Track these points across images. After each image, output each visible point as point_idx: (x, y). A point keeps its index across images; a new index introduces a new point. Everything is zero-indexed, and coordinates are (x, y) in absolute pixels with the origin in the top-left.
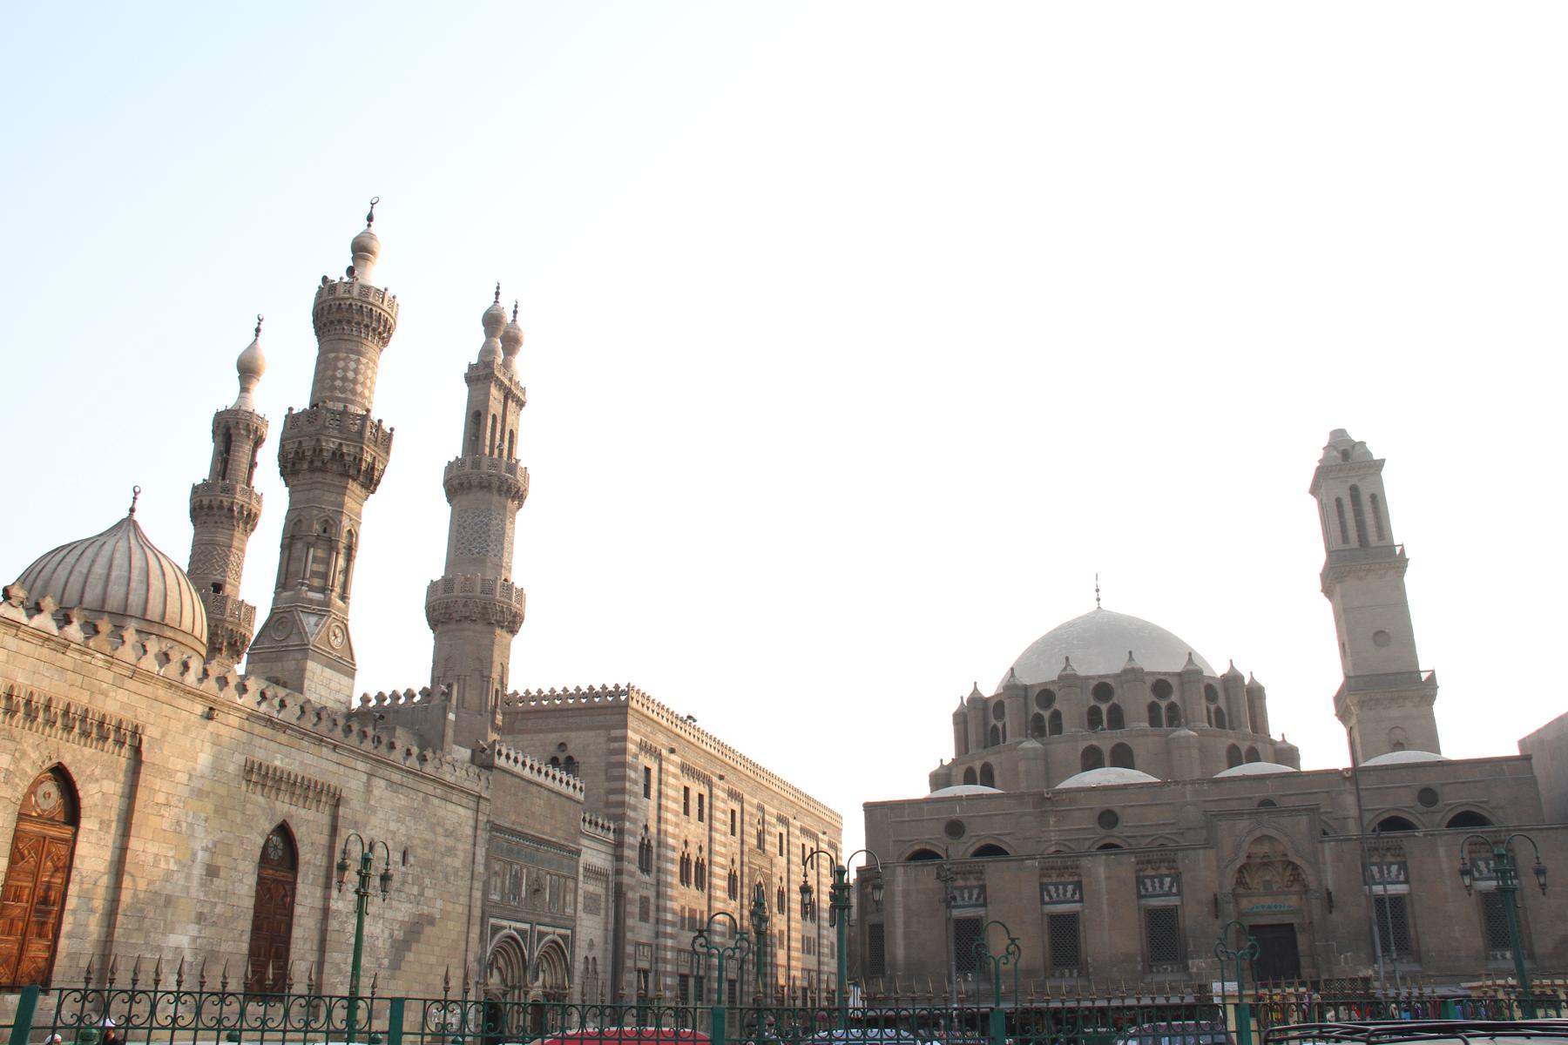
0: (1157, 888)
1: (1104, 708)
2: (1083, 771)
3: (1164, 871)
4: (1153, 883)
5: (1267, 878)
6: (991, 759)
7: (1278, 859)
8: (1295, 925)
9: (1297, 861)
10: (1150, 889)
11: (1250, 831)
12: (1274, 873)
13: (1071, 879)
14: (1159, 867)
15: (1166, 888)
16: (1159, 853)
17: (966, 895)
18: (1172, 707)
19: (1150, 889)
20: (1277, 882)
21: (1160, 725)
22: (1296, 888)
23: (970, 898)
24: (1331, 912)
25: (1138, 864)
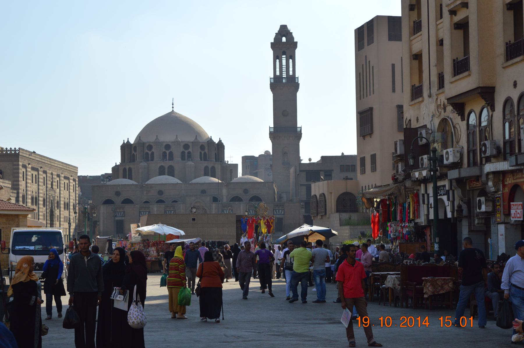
1: (168, 152)
2: (159, 176)
3: (172, 209)
6: (132, 166)
9: (206, 208)
13: (147, 211)
17: (120, 214)
18: (189, 153)
21: (185, 160)
23: (121, 214)
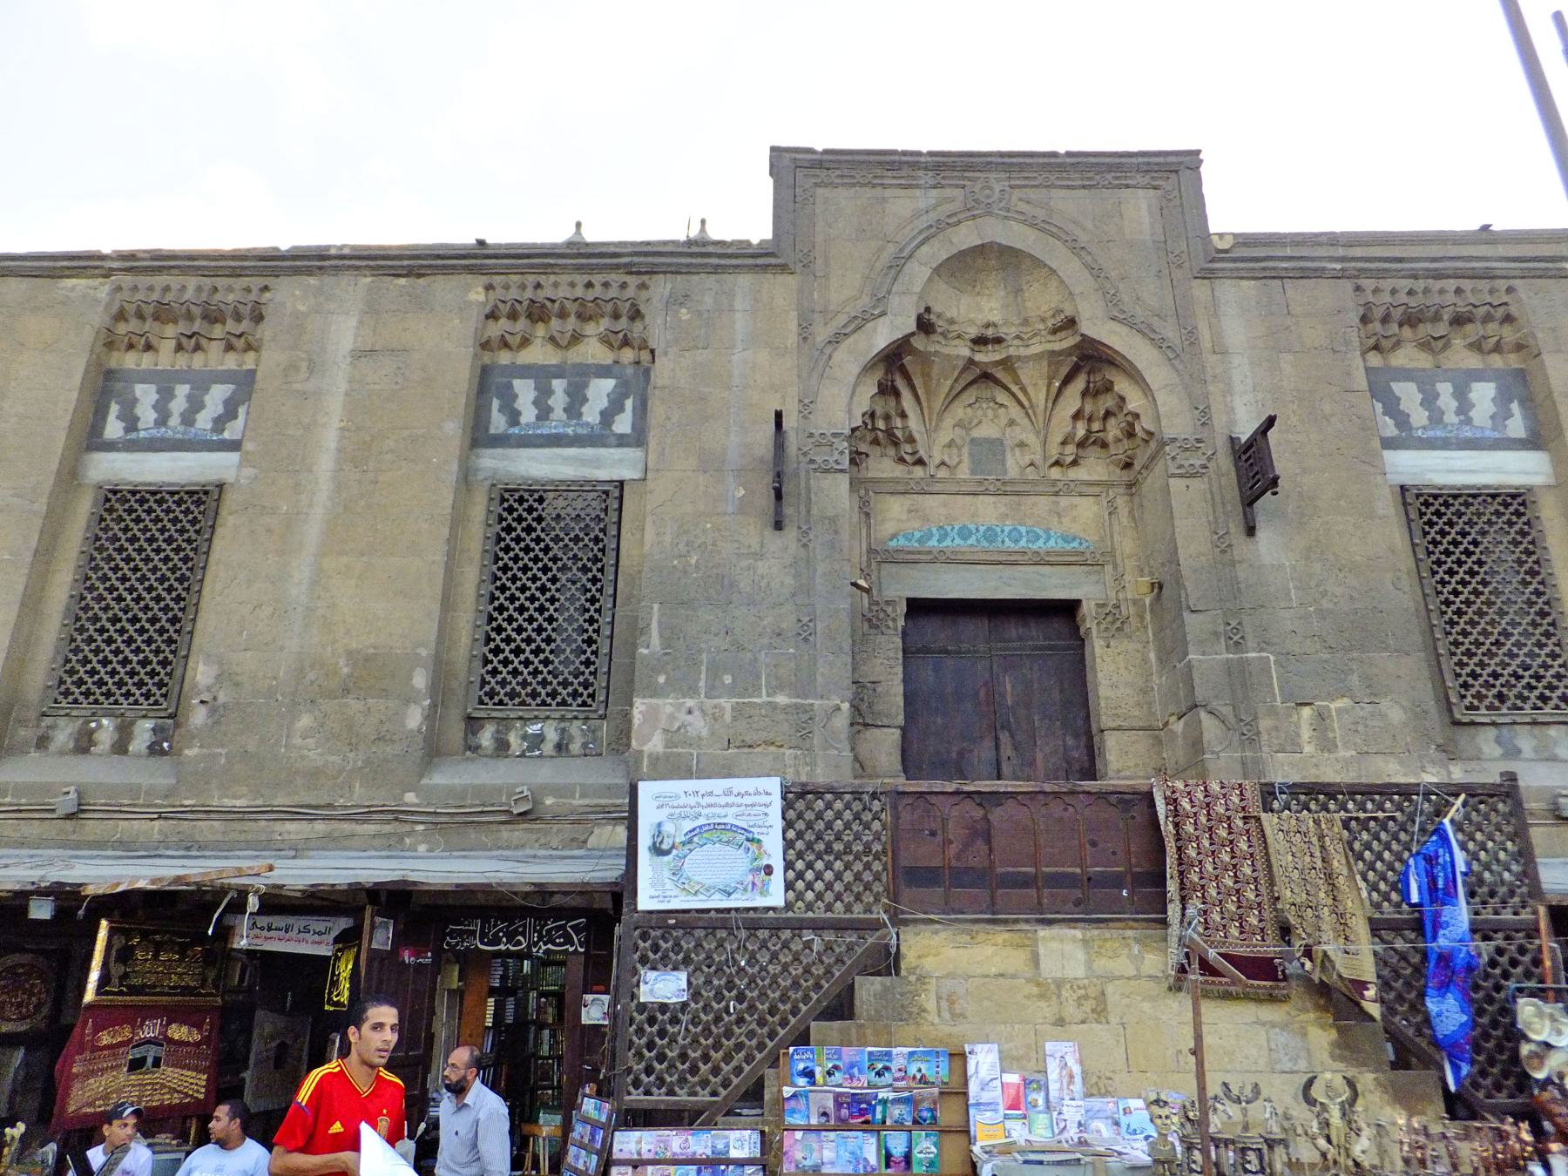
0: (559, 414)
3: (593, 351)
4: (544, 393)
5: (987, 431)
7: (1036, 349)
8: (1087, 609)
10: (528, 414)
11: (940, 228)
12: (1015, 411)
14: (576, 338)
15: (591, 414)
16: (581, 279)
19: (528, 414)
20: (1022, 445)
22: (1095, 468)
24: (1251, 531)
25: (492, 316)
